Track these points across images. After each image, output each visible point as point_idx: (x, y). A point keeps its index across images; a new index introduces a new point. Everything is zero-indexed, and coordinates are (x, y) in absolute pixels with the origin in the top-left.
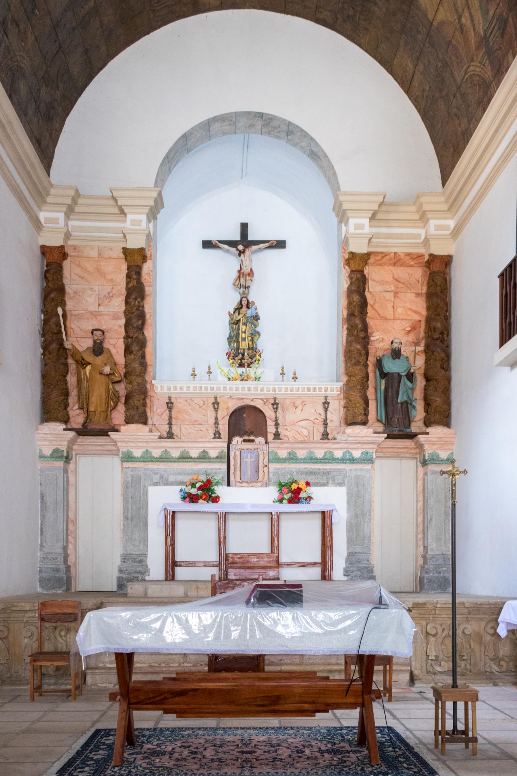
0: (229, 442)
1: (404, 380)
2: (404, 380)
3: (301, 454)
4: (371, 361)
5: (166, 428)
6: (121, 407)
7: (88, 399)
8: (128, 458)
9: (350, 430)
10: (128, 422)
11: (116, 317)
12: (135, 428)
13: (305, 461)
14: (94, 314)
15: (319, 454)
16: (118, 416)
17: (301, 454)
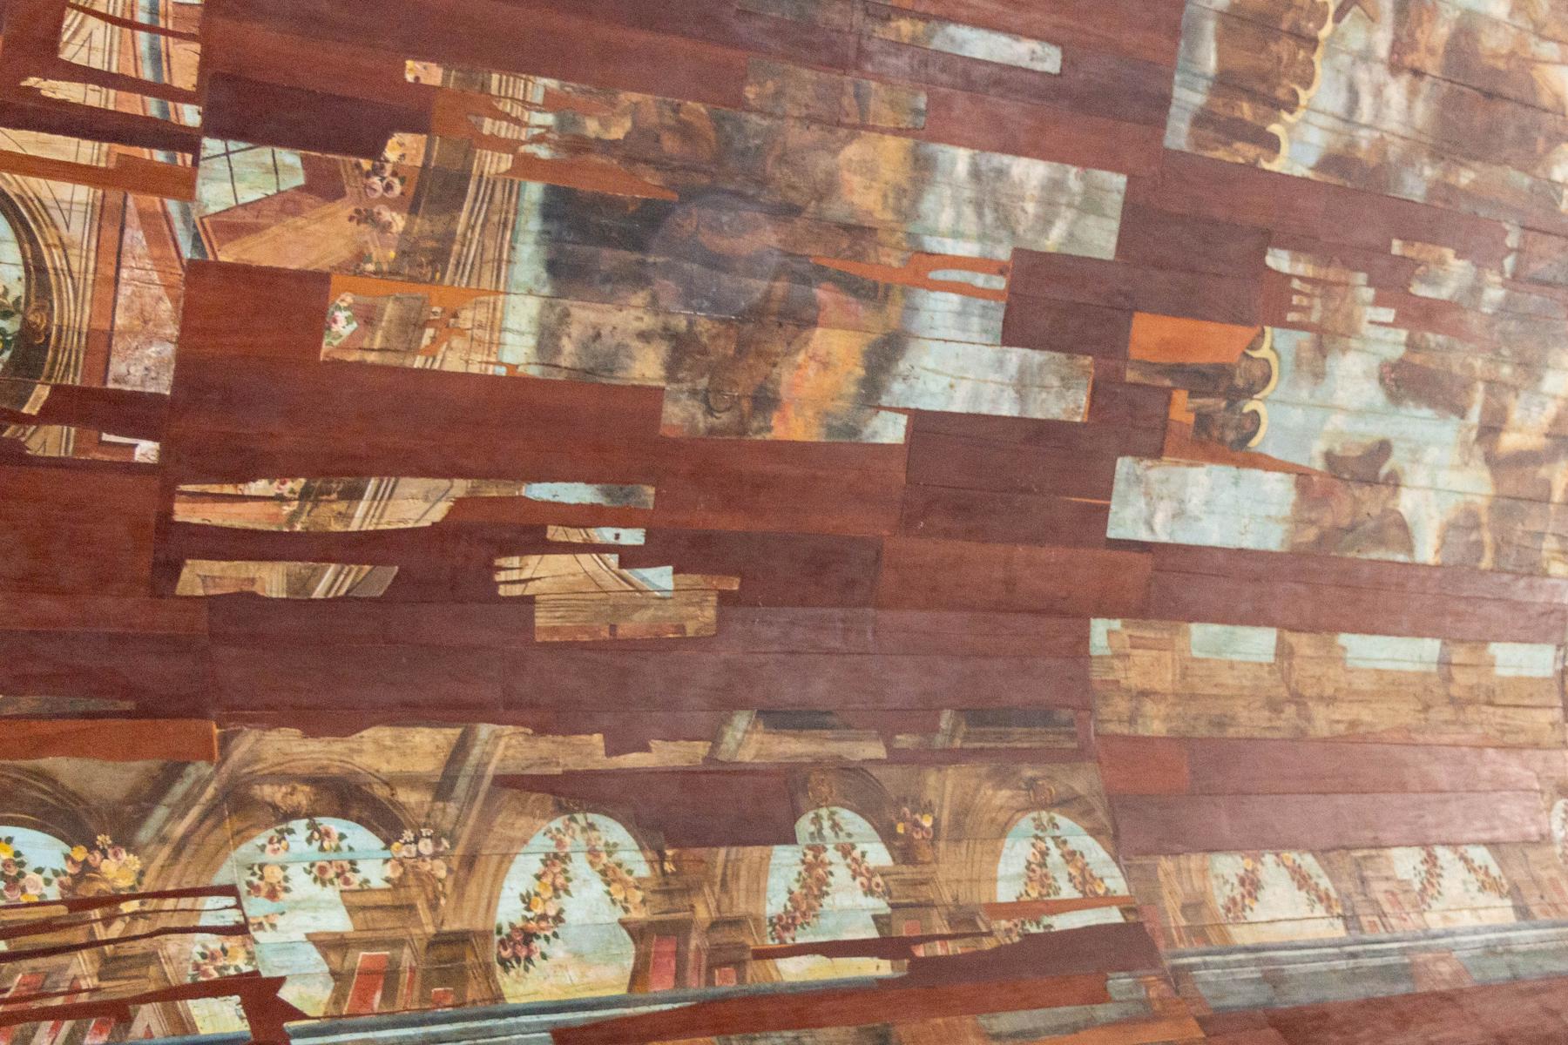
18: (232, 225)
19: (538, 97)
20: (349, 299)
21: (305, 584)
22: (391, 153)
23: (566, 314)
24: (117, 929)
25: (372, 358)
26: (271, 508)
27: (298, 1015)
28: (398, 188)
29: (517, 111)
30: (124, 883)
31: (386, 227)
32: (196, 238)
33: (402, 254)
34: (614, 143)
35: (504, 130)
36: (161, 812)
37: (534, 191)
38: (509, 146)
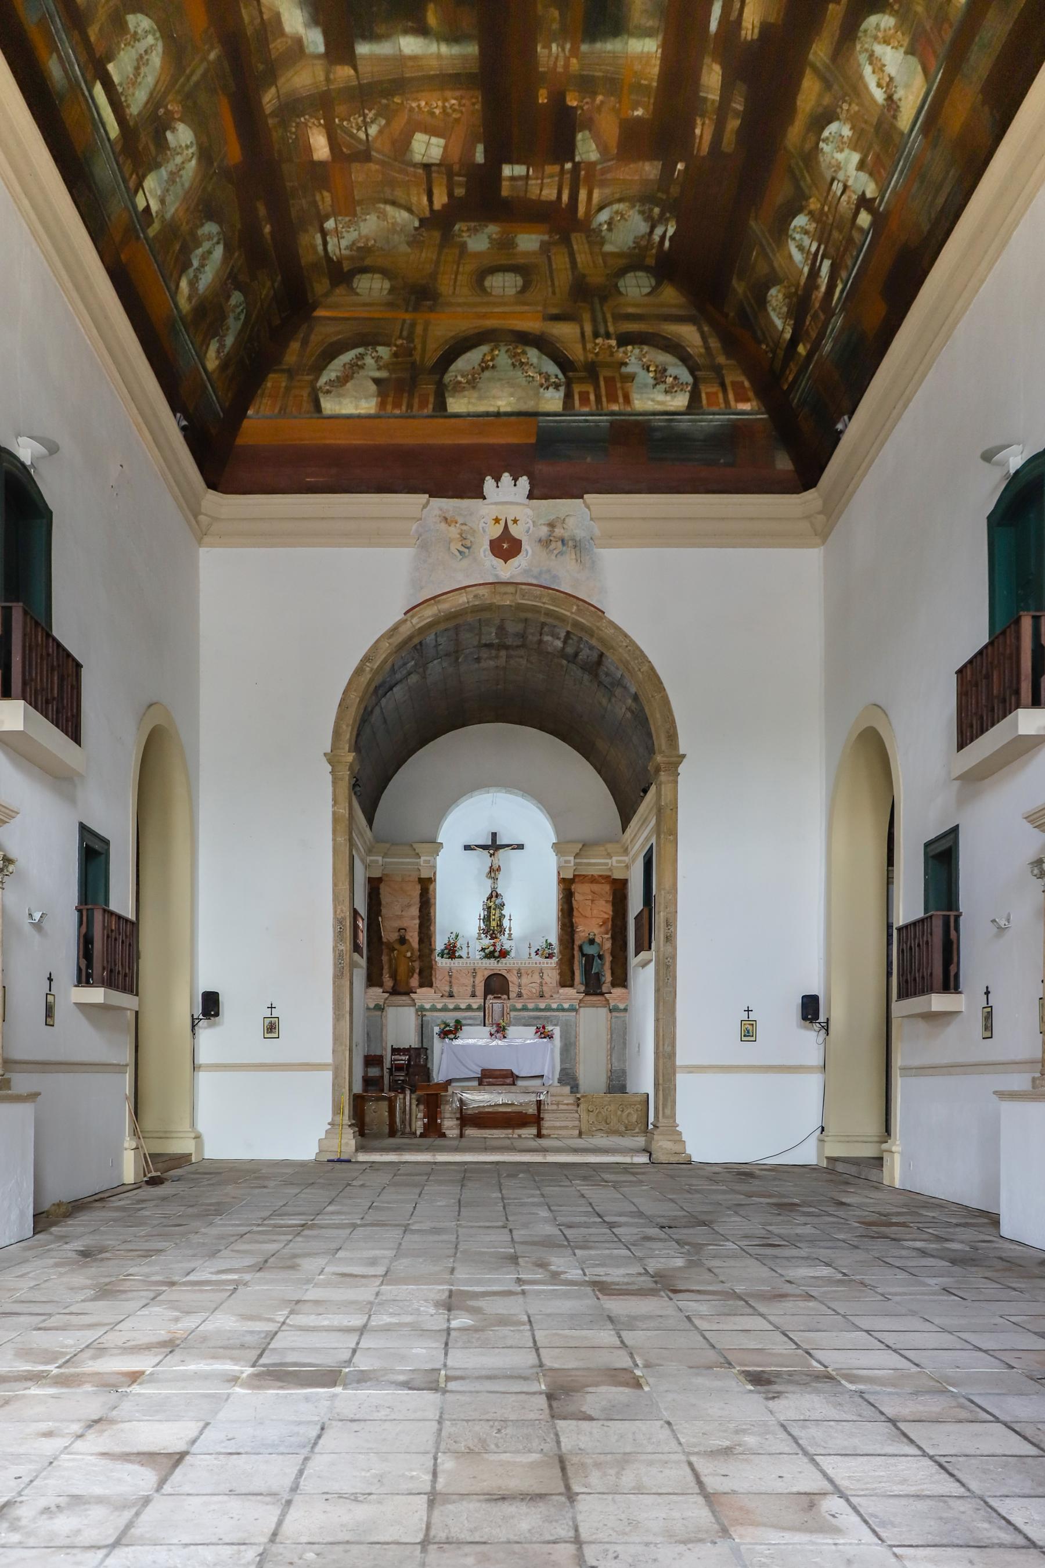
0: (485, 999)
1: (596, 958)
2: (596, 958)
3: (531, 1006)
4: (576, 948)
5: (447, 989)
6: (416, 976)
7: (396, 971)
8: (422, 1009)
9: (562, 990)
10: (421, 986)
11: (413, 918)
12: (424, 989)
13: (533, 1010)
14: (400, 917)
15: (542, 1006)
16: (414, 981)
17: (531, 1006)
18: (603, 149)
19: (546, 51)
20: (630, 112)
21: (737, 113)
22: (575, 104)
23: (636, 27)
24: (831, 218)
25: (652, 101)
26: (706, 127)
27: (874, 199)
28: (588, 100)
29: (553, 59)
30: (819, 206)
31: (602, 102)
32: (609, 160)
33: (612, 95)
34: (560, 15)
35: (561, 63)
36: (802, 184)
37: (584, 48)
38: (567, 59)
